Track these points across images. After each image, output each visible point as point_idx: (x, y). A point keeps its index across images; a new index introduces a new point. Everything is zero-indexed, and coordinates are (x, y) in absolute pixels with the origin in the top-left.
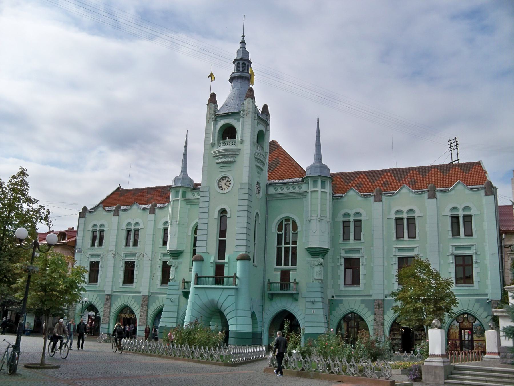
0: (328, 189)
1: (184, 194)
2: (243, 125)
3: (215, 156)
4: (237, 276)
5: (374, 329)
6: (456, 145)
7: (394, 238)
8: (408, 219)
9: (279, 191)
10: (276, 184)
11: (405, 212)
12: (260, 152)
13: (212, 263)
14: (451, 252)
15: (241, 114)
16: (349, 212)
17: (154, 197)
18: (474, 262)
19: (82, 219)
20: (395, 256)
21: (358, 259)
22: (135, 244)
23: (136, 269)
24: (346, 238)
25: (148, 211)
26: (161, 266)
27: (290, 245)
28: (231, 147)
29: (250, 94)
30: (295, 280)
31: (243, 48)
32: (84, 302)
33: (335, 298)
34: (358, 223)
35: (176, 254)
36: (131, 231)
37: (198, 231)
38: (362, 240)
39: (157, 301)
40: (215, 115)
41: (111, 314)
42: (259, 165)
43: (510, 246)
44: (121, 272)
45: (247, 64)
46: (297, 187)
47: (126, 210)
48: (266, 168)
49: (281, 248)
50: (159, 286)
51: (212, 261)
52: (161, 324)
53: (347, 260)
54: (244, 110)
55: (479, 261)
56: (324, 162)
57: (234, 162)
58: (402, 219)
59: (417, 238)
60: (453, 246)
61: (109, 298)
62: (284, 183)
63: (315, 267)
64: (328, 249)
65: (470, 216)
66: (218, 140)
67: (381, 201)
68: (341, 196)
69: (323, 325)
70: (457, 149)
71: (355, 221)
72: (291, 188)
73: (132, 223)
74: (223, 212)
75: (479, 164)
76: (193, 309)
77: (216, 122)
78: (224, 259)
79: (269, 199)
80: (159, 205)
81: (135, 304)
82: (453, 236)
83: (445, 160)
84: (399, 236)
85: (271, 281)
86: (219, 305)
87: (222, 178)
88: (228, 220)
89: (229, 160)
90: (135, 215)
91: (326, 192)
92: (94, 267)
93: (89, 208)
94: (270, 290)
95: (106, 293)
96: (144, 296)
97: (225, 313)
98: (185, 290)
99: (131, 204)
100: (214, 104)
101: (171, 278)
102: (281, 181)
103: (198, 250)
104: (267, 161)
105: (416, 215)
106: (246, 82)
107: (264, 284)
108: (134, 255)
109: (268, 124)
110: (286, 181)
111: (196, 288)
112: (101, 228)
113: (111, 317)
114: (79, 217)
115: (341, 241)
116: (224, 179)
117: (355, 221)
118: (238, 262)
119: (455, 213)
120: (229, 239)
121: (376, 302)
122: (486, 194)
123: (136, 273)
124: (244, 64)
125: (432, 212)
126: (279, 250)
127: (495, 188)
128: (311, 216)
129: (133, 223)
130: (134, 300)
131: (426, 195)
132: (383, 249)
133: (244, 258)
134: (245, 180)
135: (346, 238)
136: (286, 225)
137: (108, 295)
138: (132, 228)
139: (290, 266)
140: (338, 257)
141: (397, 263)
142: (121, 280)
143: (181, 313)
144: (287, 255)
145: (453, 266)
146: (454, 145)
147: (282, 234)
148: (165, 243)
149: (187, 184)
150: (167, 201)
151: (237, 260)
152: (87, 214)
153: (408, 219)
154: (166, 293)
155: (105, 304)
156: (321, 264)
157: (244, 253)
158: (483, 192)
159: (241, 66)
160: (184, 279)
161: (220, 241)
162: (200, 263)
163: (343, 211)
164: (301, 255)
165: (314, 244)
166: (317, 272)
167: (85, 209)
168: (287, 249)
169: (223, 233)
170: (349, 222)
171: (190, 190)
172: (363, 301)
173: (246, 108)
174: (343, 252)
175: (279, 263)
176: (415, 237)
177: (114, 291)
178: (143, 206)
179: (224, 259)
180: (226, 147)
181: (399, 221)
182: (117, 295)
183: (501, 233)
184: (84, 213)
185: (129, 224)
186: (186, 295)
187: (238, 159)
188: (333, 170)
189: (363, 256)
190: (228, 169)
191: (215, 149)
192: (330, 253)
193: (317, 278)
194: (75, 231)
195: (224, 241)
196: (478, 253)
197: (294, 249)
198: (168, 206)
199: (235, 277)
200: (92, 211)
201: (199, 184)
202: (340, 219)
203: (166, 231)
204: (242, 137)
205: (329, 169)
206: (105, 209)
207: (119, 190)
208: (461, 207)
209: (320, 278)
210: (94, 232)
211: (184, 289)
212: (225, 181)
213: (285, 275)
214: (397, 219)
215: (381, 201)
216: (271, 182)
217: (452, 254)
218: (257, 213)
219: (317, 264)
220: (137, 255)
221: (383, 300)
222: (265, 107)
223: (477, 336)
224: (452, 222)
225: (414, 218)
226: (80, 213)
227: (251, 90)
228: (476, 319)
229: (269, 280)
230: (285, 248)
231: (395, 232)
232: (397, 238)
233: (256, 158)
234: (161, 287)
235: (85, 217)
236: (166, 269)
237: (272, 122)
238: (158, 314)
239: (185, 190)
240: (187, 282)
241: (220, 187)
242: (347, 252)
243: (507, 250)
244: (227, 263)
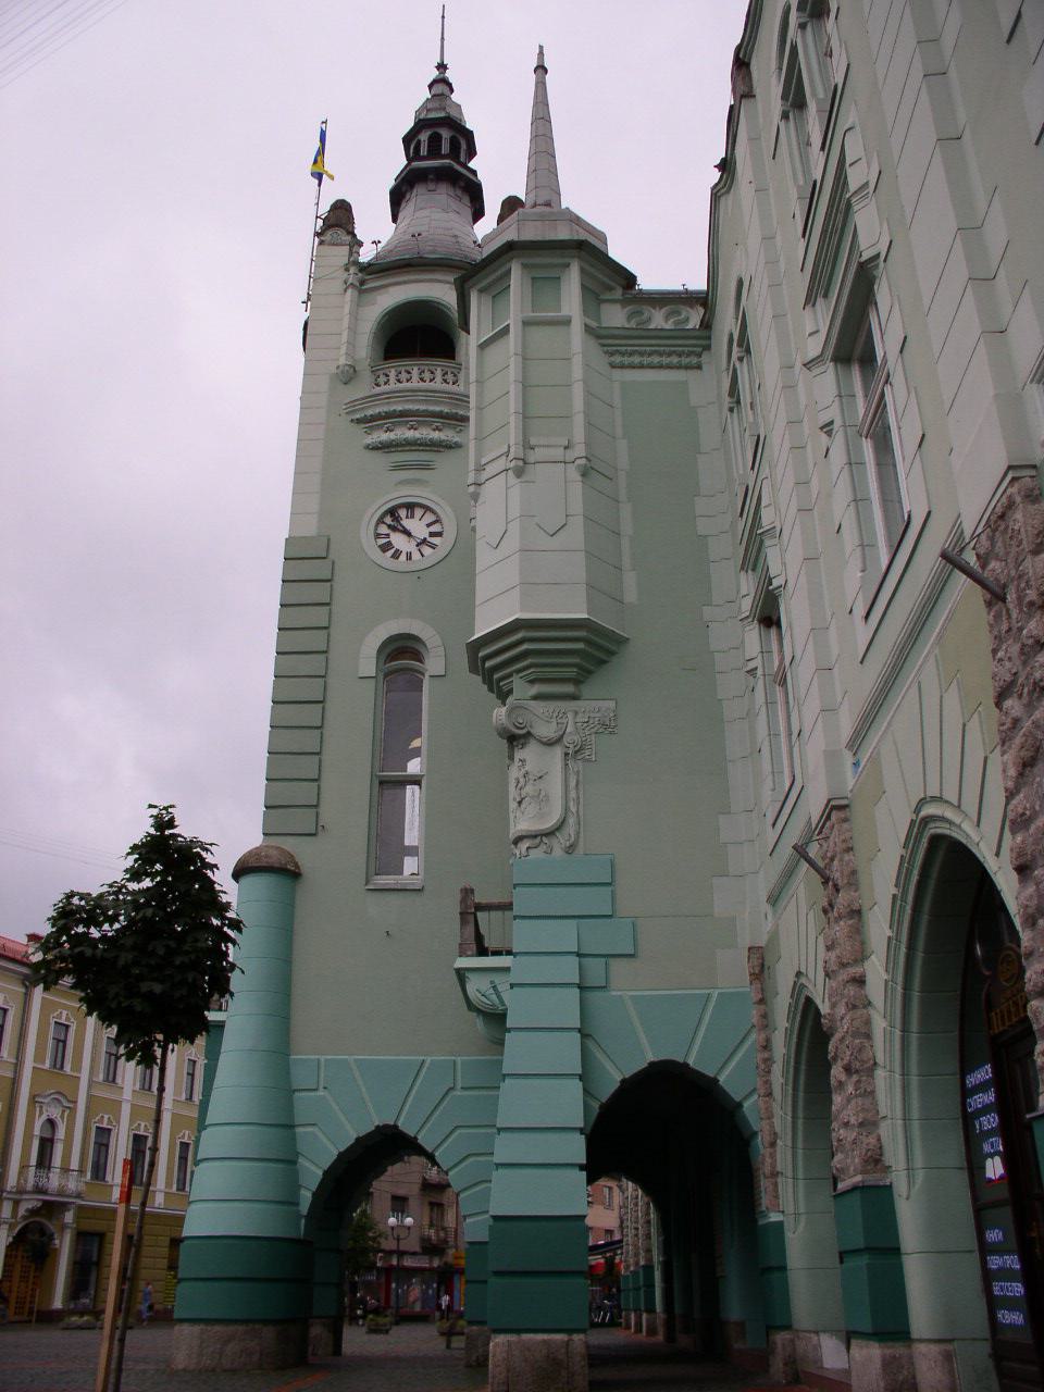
3: (359, 421)
45: (464, 146)
57: (457, 446)
87: (392, 512)
89: (436, 435)
116: (403, 513)
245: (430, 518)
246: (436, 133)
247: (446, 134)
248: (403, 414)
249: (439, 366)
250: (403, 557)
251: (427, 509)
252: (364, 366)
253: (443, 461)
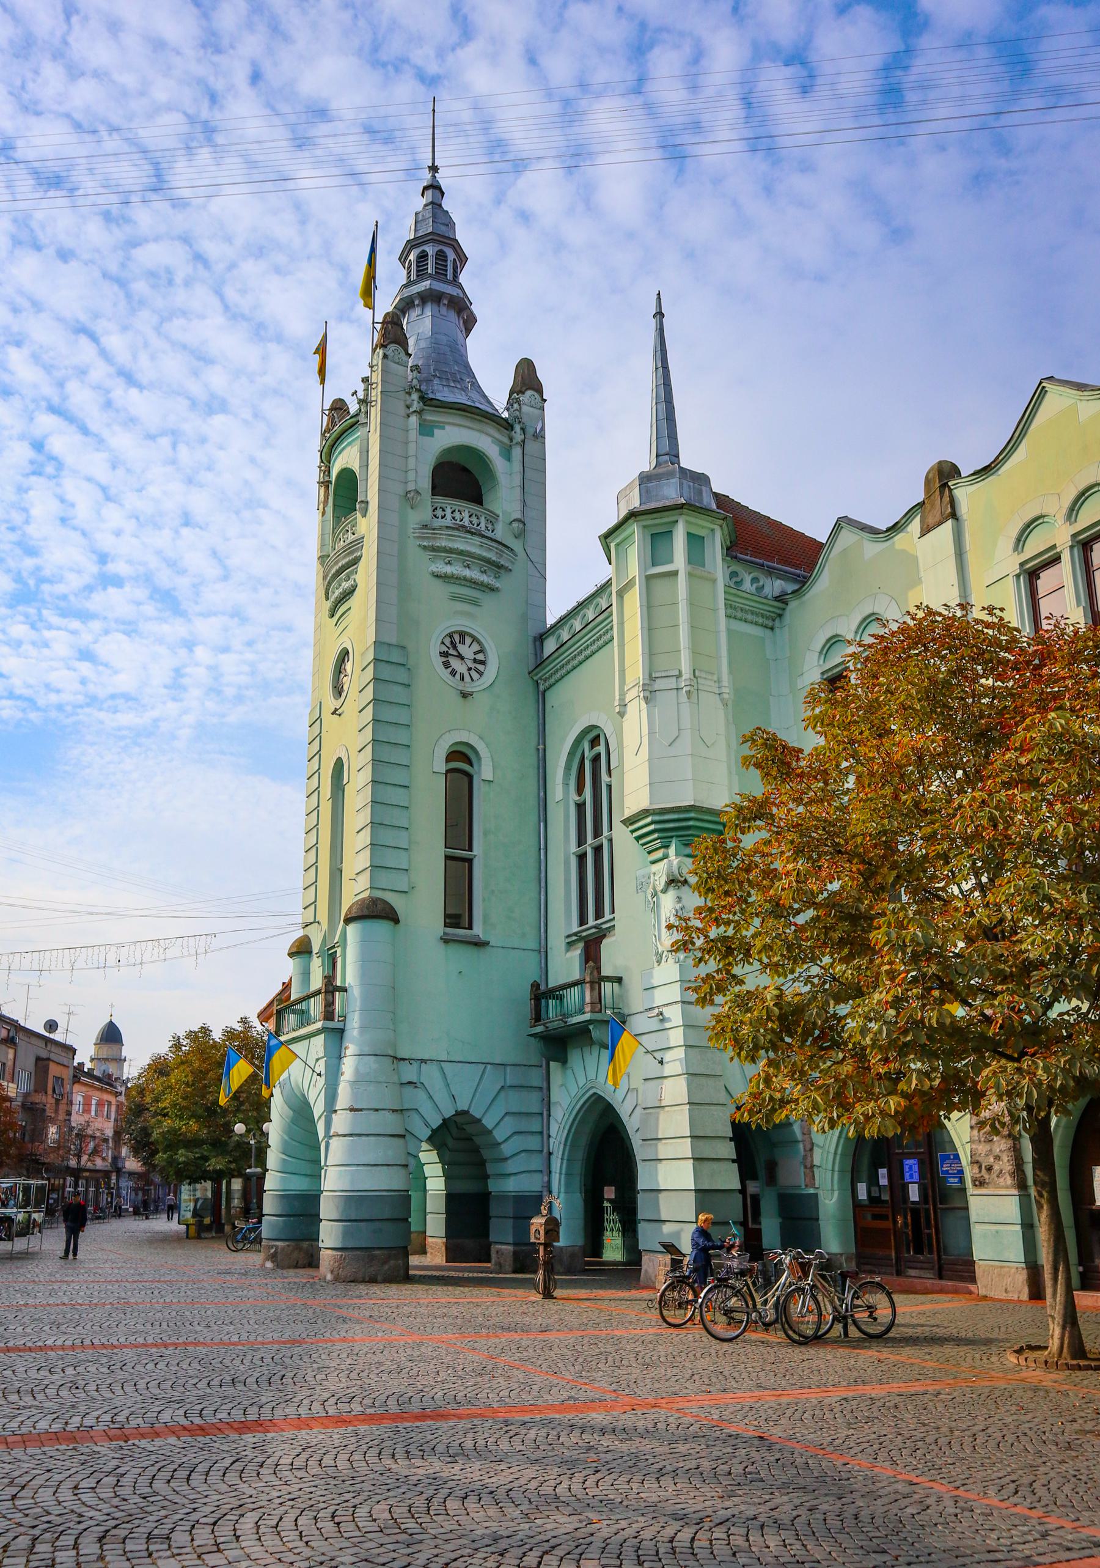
31: (436, 206)
57: (493, 590)
87: (451, 635)
89: (484, 578)
118: (352, 930)
161: (448, 858)
162: (381, 928)
241: (447, 665)
245: (476, 647)
246: (441, 251)
247: (451, 255)
248: (461, 553)
250: (458, 676)
251: (475, 639)
253: (487, 600)
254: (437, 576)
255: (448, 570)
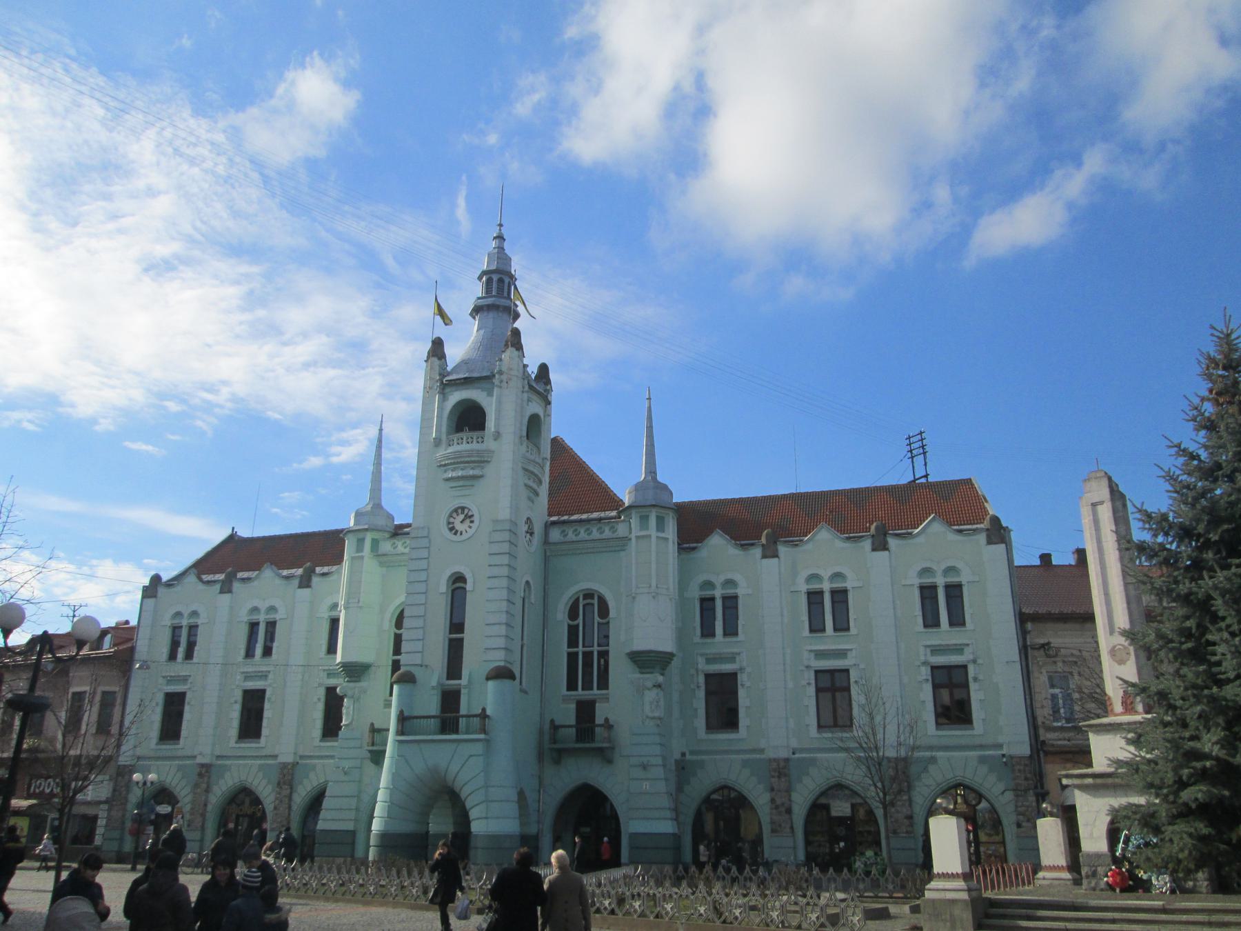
0: (671, 531)
1: (375, 543)
2: (499, 402)
4: (488, 712)
5: (772, 822)
6: (923, 447)
7: (806, 632)
8: (834, 592)
9: (571, 536)
10: (564, 522)
11: (826, 578)
12: (532, 457)
13: (433, 688)
14: (922, 658)
15: (496, 381)
16: (713, 579)
17: (311, 553)
18: (970, 679)
19: (151, 601)
20: (808, 667)
21: (733, 676)
22: (267, 652)
23: (267, 706)
24: (708, 631)
25: (296, 582)
26: (323, 699)
27: (596, 649)
28: (475, 446)
29: (515, 340)
30: (607, 720)
31: (501, 249)
32: (149, 784)
33: (688, 757)
34: (731, 602)
35: (355, 671)
36: (257, 624)
37: (405, 621)
38: (741, 637)
39: (312, 775)
40: (443, 382)
41: (210, 807)
42: (531, 483)
43: (1043, 646)
44: (235, 714)
45: (507, 280)
46: (607, 529)
47: (249, 579)
48: (544, 490)
49: (577, 654)
50: (317, 742)
51: (434, 683)
52: (321, 825)
53: (708, 676)
54: (500, 372)
55: (981, 677)
56: (659, 478)
57: (482, 476)
58: (821, 593)
59: (853, 630)
60: (926, 646)
61: (205, 771)
62: (581, 521)
63: (647, 692)
64: (670, 656)
65: (959, 586)
66: (449, 433)
67: (777, 556)
68: (694, 549)
69: (668, 814)
70: (924, 453)
71: (724, 598)
72: (595, 530)
73: (259, 606)
74: (459, 579)
75: (968, 482)
76: (393, 790)
77: (444, 397)
78: (460, 678)
79: (549, 554)
80: (318, 570)
81: (264, 782)
82: (926, 626)
83: (900, 476)
84: (816, 627)
85: (557, 723)
86: (450, 777)
87: (456, 510)
88: (468, 595)
89: (471, 472)
90: (267, 590)
91: (666, 539)
92: (174, 706)
93: (165, 577)
94: (555, 742)
95: (200, 760)
96: (284, 766)
97: (463, 795)
98: (375, 748)
99: (258, 567)
100: (440, 359)
101: (344, 722)
102: (575, 517)
103: (403, 658)
104: (546, 479)
105: (848, 585)
106: (505, 316)
107: (541, 732)
108: (264, 676)
109: (549, 403)
110: (584, 516)
111: (400, 742)
112: (191, 621)
113: (208, 815)
114: (143, 597)
115: (697, 638)
117: (724, 598)
118: (491, 683)
119: (927, 580)
120: (470, 637)
121: (774, 765)
122: (990, 542)
123: (267, 714)
124: (501, 281)
125: (880, 580)
126: (572, 658)
127: (1006, 529)
128: (637, 587)
129: (263, 606)
130: (261, 774)
131: (867, 544)
132: (784, 654)
133: (502, 674)
134: (504, 513)
135: (708, 631)
136: (584, 606)
137: (202, 765)
138: (262, 618)
139: (595, 691)
140: (693, 671)
141: (813, 682)
142: (234, 731)
143: (366, 798)
144: (587, 668)
145: (928, 688)
146: (917, 447)
147: (577, 626)
148: (332, 649)
149: (381, 522)
150: (338, 559)
151: (488, 679)
152: (161, 591)
153: (834, 592)
154: (332, 757)
155: (196, 785)
156: (659, 686)
157: (502, 664)
158: (982, 538)
159: (495, 285)
160: (372, 724)
161: (451, 640)
162: (409, 686)
163: (702, 578)
164: (620, 670)
165: (642, 643)
166: (651, 703)
167: (156, 579)
168: (588, 656)
169: (457, 626)
170: (713, 599)
171: (387, 535)
172: (745, 763)
173: (504, 369)
174: (701, 662)
175: (572, 685)
176: (848, 629)
177: (218, 757)
178: (285, 572)
179: (460, 678)
180: (465, 447)
181: (814, 597)
182: (225, 766)
183: (1023, 619)
184: (154, 588)
185: (255, 610)
186: (377, 757)
187: (489, 470)
188: (678, 498)
189: (742, 669)
190: (467, 492)
191: (442, 452)
192: (675, 663)
193: (650, 715)
194: (133, 628)
195: (462, 640)
196: (980, 661)
197: (604, 655)
198: (339, 572)
199: (483, 715)
200: (170, 584)
201: (409, 525)
202: (695, 593)
203: (334, 622)
204: (497, 425)
205: (671, 493)
206: (201, 580)
207: (232, 539)
208: (939, 568)
209: (657, 714)
210: (176, 629)
211: (373, 744)
212: (462, 517)
213: (586, 710)
214: (810, 594)
215: (777, 556)
216: (554, 518)
217: (925, 663)
218: (527, 582)
219: (649, 684)
220: (271, 676)
221: (787, 760)
222: (544, 369)
223: (987, 834)
224: (923, 598)
225: (844, 592)
226: (145, 589)
227: (516, 333)
228: (980, 797)
229: (552, 721)
230: (584, 653)
231: (805, 618)
232: (811, 631)
233: (526, 470)
234: (322, 744)
235: (155, 597)
236: (333, 703)
237: (554, 397)
238: (316, 803)
239: (376, 535)
240: (379, 731)
241: (451, 529)
242: (709, 661)
243: (1036, 653)
244: (466, 687)
249: (475, 434)
252: (444, 437)
254: (448, 480)
255: (454, 474)
